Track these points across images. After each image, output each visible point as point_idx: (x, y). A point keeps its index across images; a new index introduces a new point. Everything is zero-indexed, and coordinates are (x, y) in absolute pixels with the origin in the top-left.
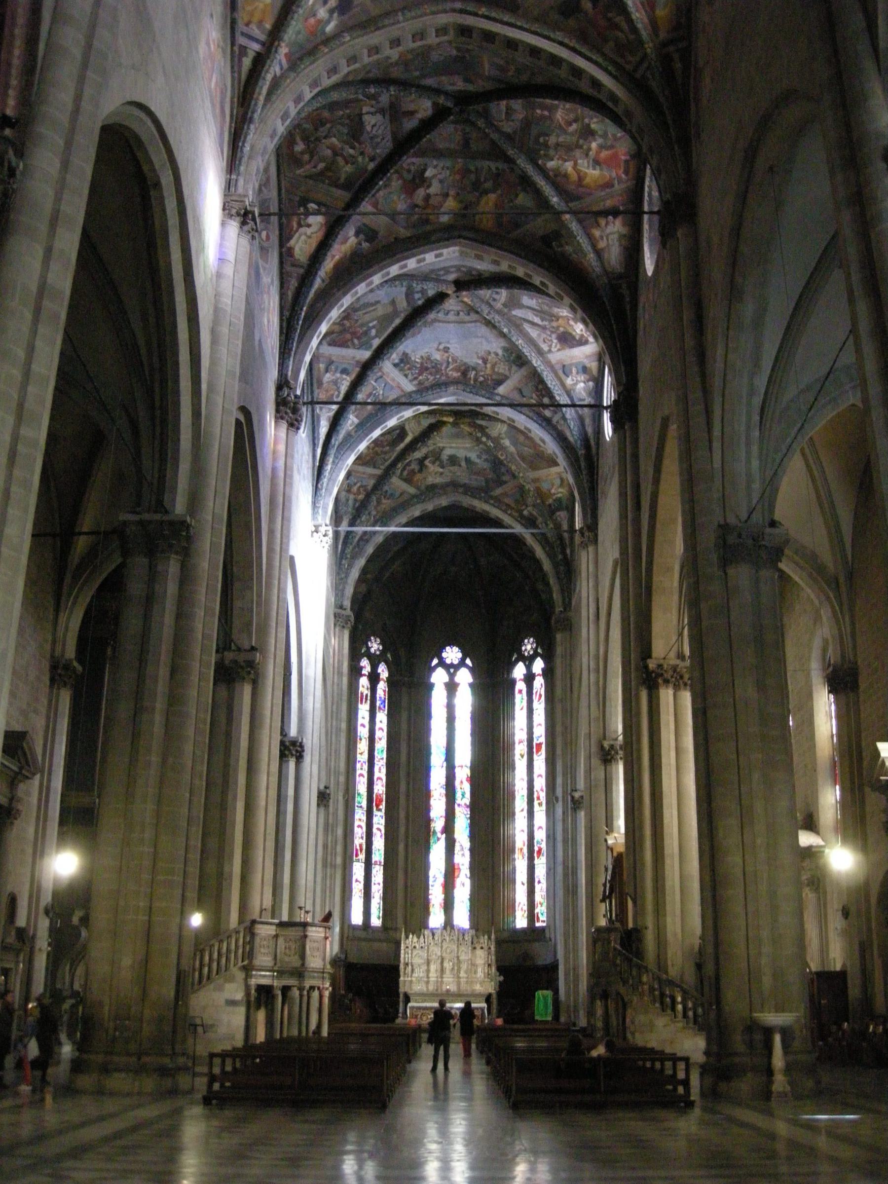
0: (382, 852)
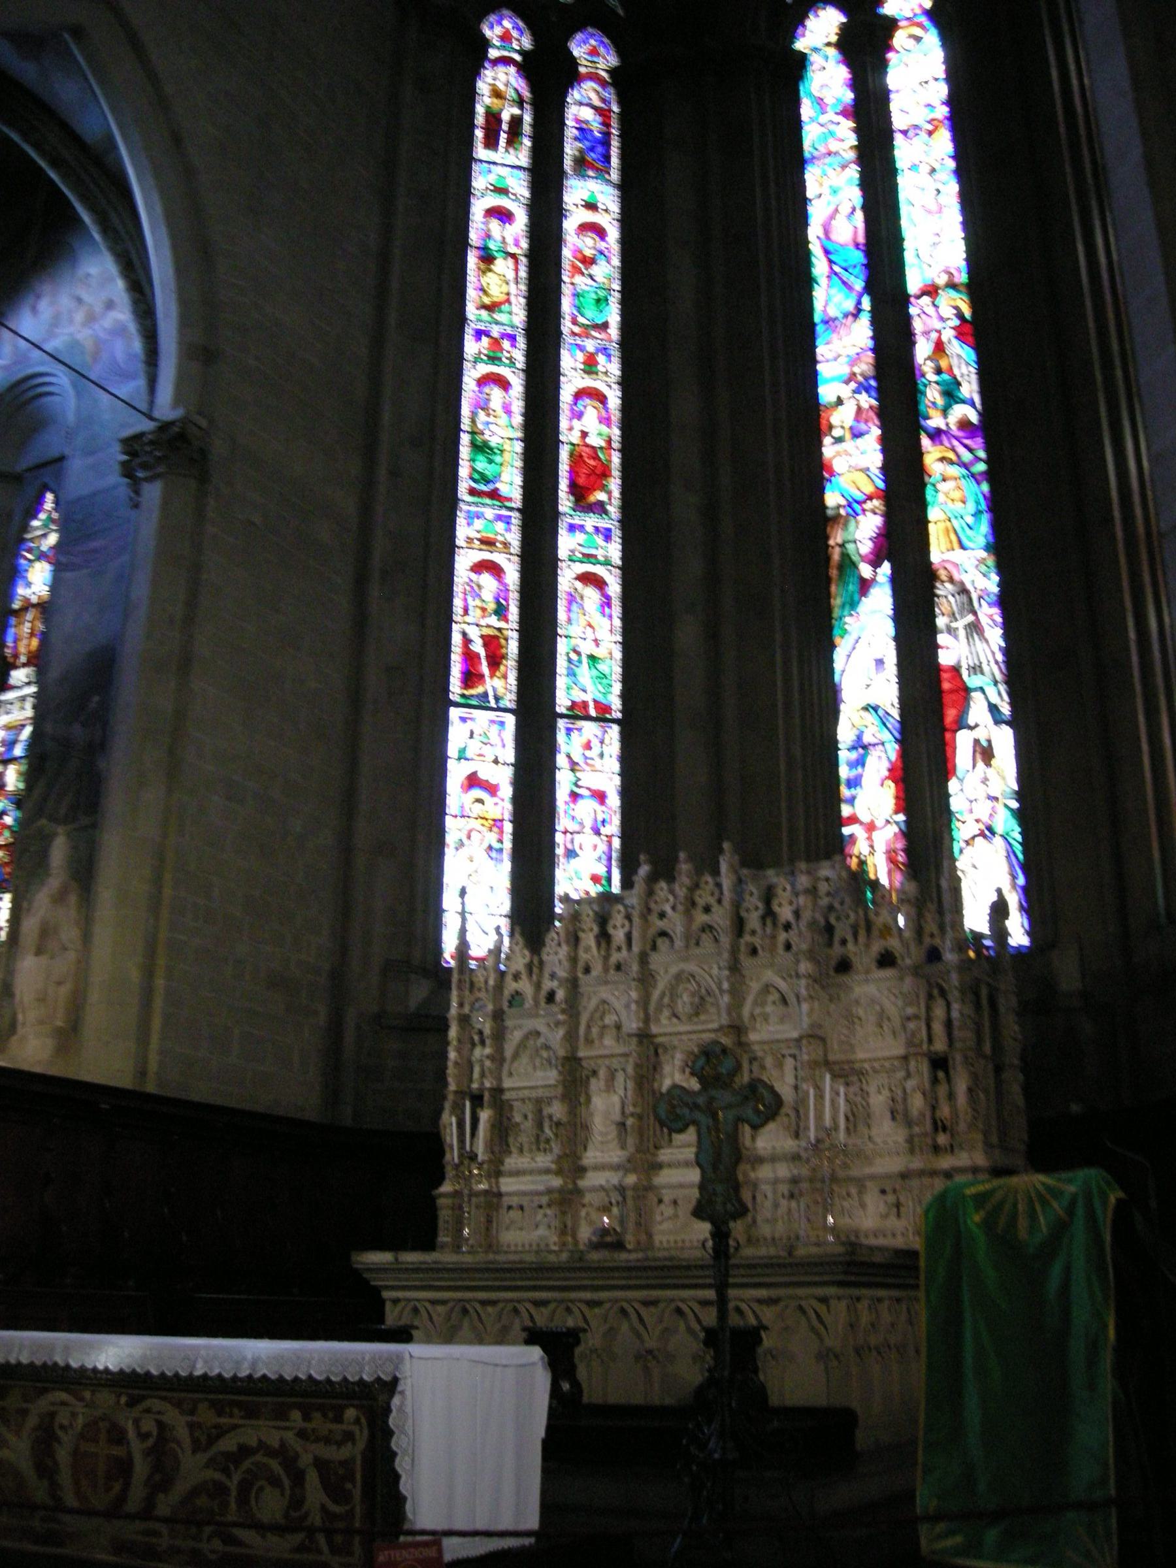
0: (614, 668)
